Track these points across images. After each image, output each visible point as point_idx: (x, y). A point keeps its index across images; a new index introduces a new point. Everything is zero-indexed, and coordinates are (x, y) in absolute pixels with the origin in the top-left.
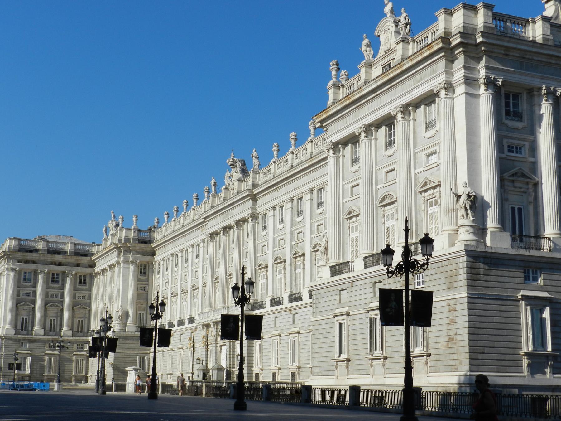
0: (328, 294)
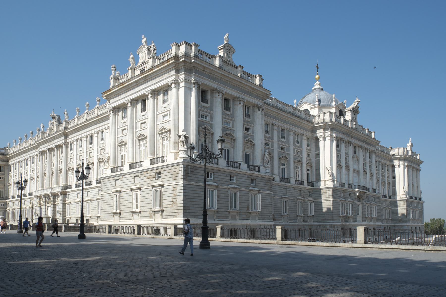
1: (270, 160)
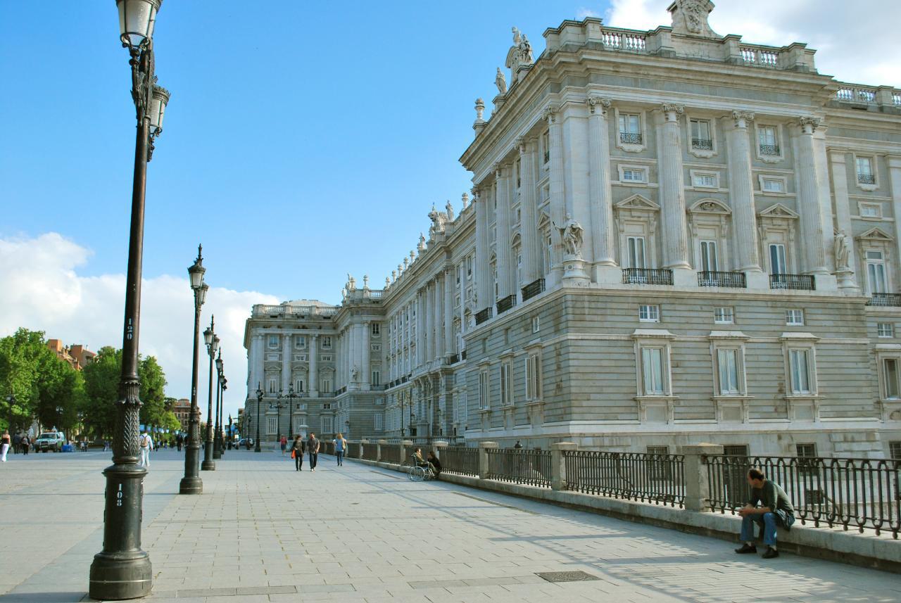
0: (476, 344)
1: (886, 252)
